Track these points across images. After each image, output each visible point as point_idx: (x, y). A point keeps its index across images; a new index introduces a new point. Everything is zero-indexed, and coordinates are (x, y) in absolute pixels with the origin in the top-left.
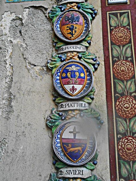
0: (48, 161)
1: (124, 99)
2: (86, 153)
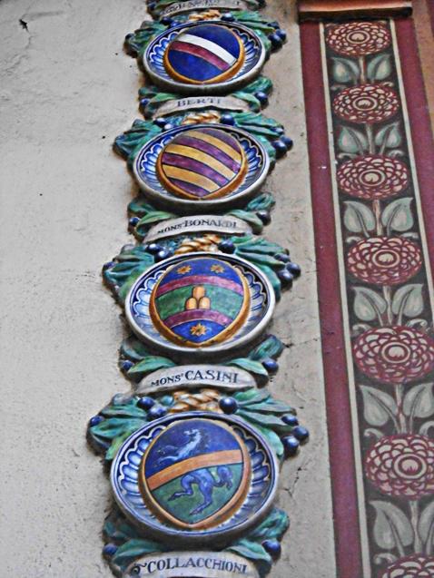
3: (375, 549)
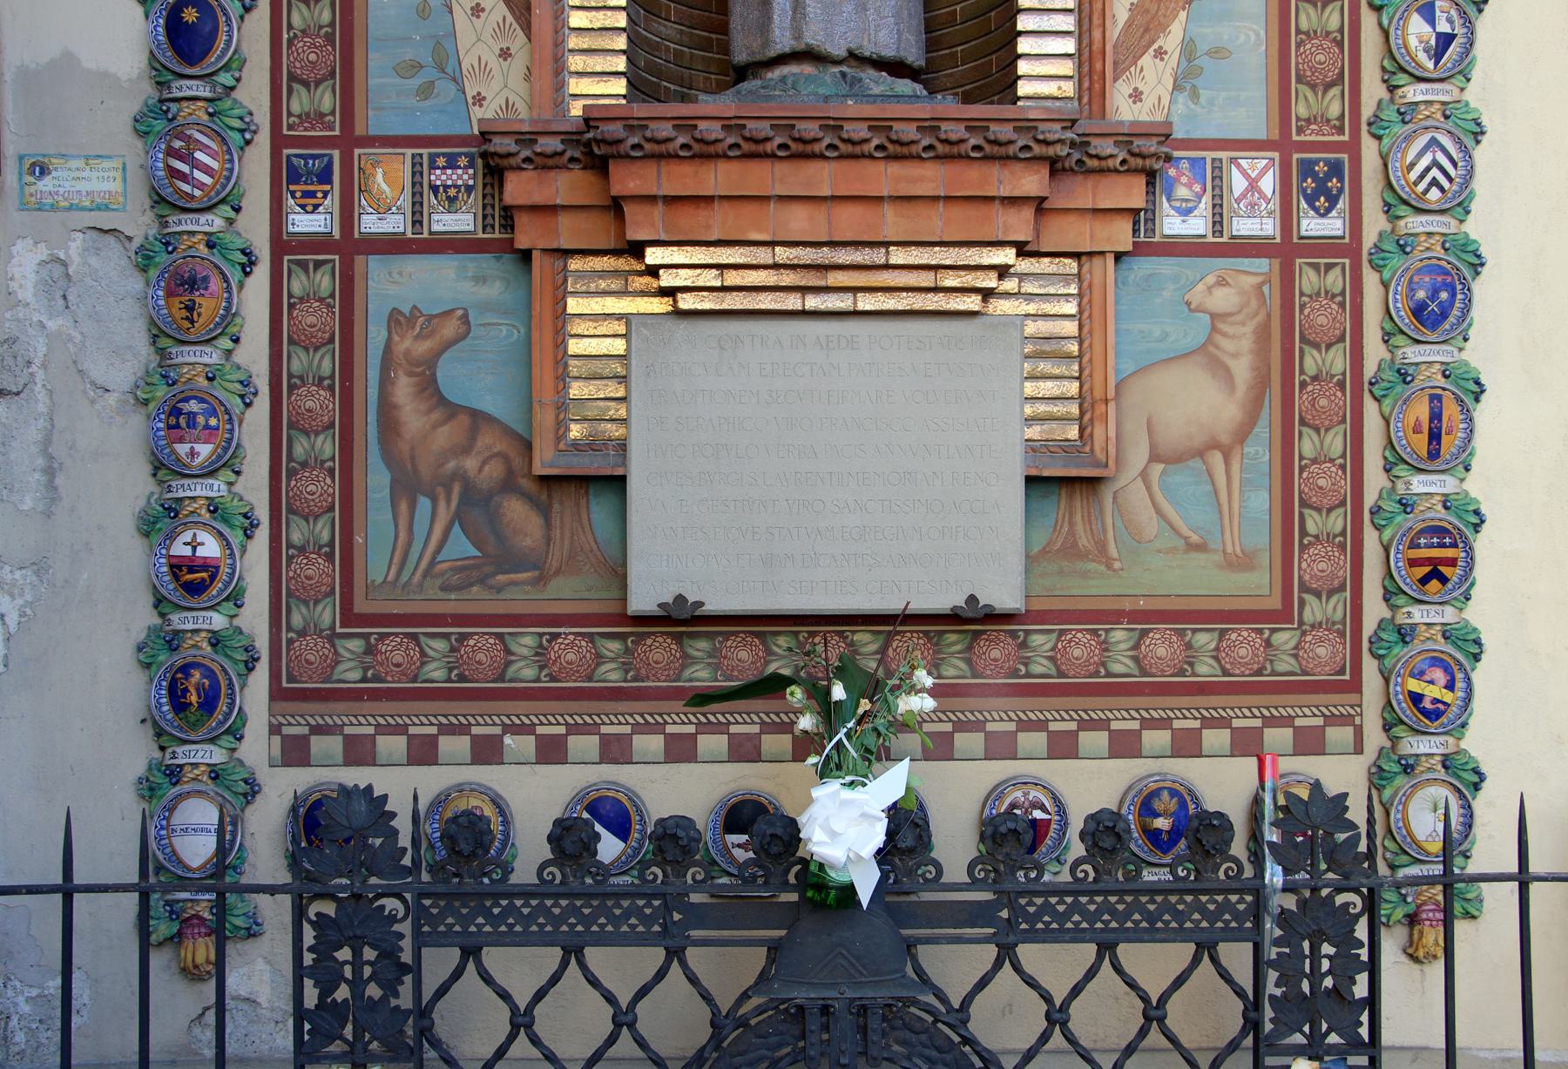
1: (307, 474)
2: (220, 585)
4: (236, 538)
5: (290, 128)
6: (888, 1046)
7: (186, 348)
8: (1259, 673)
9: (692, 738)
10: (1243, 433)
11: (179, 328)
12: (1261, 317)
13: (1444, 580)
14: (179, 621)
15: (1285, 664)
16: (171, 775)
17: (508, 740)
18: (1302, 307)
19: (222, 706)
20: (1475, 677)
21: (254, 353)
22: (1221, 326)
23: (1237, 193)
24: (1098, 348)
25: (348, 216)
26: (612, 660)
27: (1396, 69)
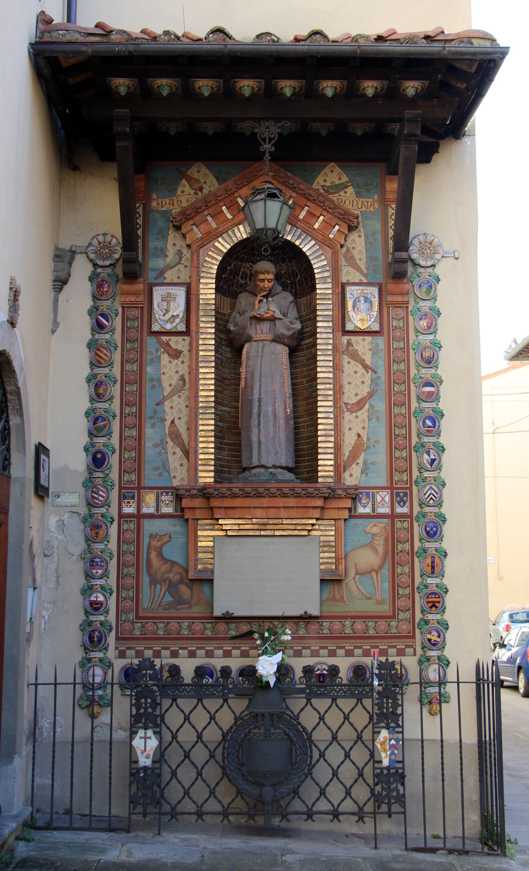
0: (82, 612)
3: (125, 436)
4: (108, 595)
5: (124, 484)
6: (279, 725)
7: (95, 544)
8: (387, 633)
9: (230, 651)
10: (381, 567)
11: (94, 539)
12: (385, 535)
13: (436, 607)
14: (92, 618)
15: (394, 631)
16: (88, 661)
17: (180, 651)
18: (397, 532)
19: (103, 642)
20: (446, 635)
21: (113, 545)
22: (375, 537)
23: (378, 501)
24: (340, 544)
25: (139, 508)
26: (209, 629)
27: (421, 468)
